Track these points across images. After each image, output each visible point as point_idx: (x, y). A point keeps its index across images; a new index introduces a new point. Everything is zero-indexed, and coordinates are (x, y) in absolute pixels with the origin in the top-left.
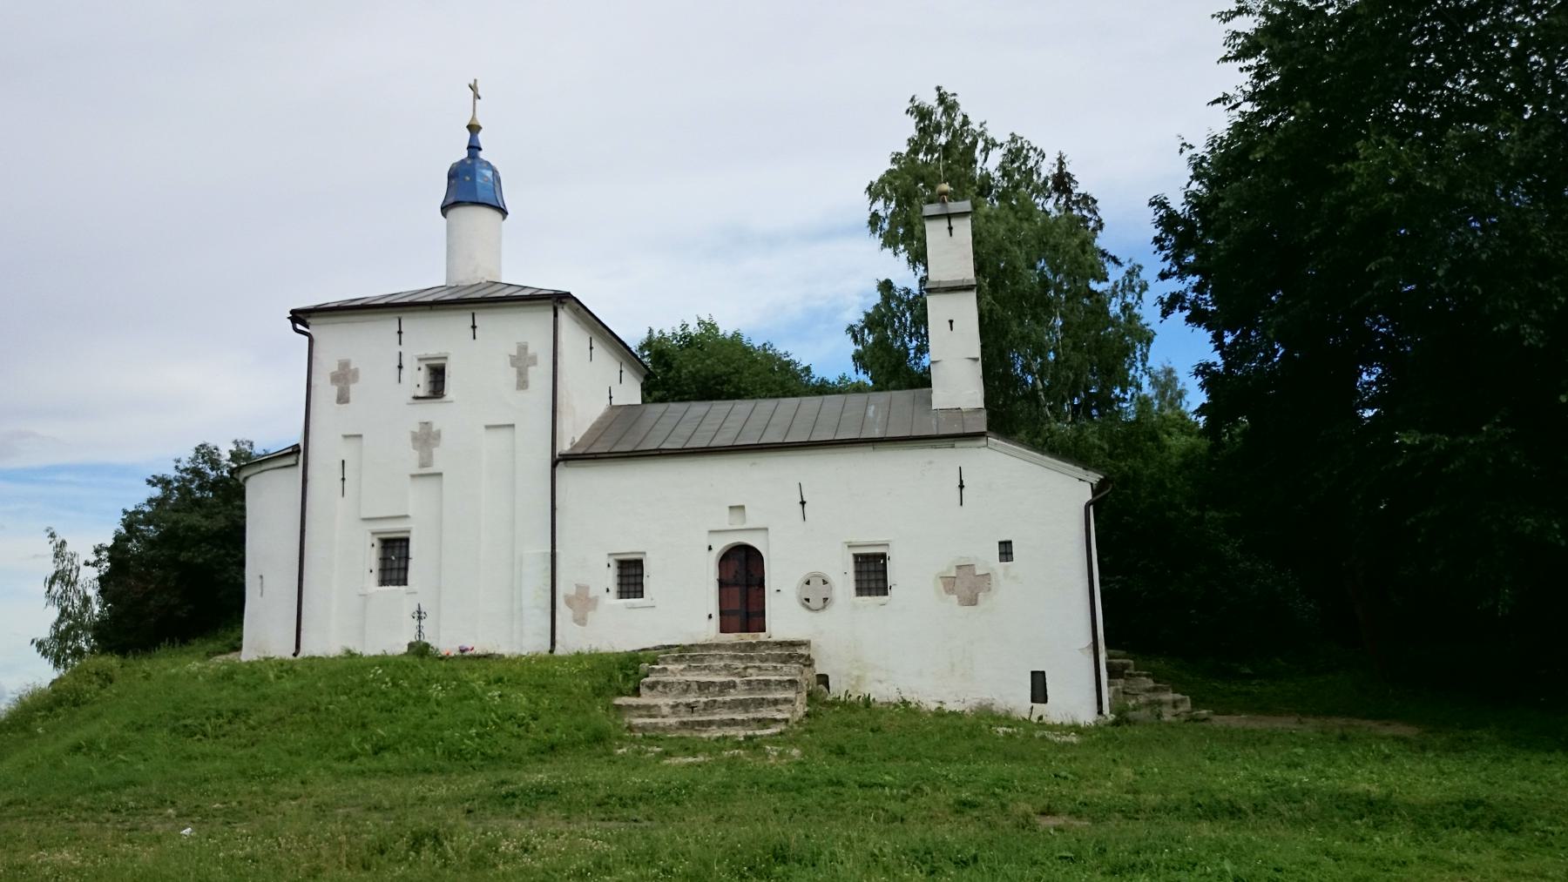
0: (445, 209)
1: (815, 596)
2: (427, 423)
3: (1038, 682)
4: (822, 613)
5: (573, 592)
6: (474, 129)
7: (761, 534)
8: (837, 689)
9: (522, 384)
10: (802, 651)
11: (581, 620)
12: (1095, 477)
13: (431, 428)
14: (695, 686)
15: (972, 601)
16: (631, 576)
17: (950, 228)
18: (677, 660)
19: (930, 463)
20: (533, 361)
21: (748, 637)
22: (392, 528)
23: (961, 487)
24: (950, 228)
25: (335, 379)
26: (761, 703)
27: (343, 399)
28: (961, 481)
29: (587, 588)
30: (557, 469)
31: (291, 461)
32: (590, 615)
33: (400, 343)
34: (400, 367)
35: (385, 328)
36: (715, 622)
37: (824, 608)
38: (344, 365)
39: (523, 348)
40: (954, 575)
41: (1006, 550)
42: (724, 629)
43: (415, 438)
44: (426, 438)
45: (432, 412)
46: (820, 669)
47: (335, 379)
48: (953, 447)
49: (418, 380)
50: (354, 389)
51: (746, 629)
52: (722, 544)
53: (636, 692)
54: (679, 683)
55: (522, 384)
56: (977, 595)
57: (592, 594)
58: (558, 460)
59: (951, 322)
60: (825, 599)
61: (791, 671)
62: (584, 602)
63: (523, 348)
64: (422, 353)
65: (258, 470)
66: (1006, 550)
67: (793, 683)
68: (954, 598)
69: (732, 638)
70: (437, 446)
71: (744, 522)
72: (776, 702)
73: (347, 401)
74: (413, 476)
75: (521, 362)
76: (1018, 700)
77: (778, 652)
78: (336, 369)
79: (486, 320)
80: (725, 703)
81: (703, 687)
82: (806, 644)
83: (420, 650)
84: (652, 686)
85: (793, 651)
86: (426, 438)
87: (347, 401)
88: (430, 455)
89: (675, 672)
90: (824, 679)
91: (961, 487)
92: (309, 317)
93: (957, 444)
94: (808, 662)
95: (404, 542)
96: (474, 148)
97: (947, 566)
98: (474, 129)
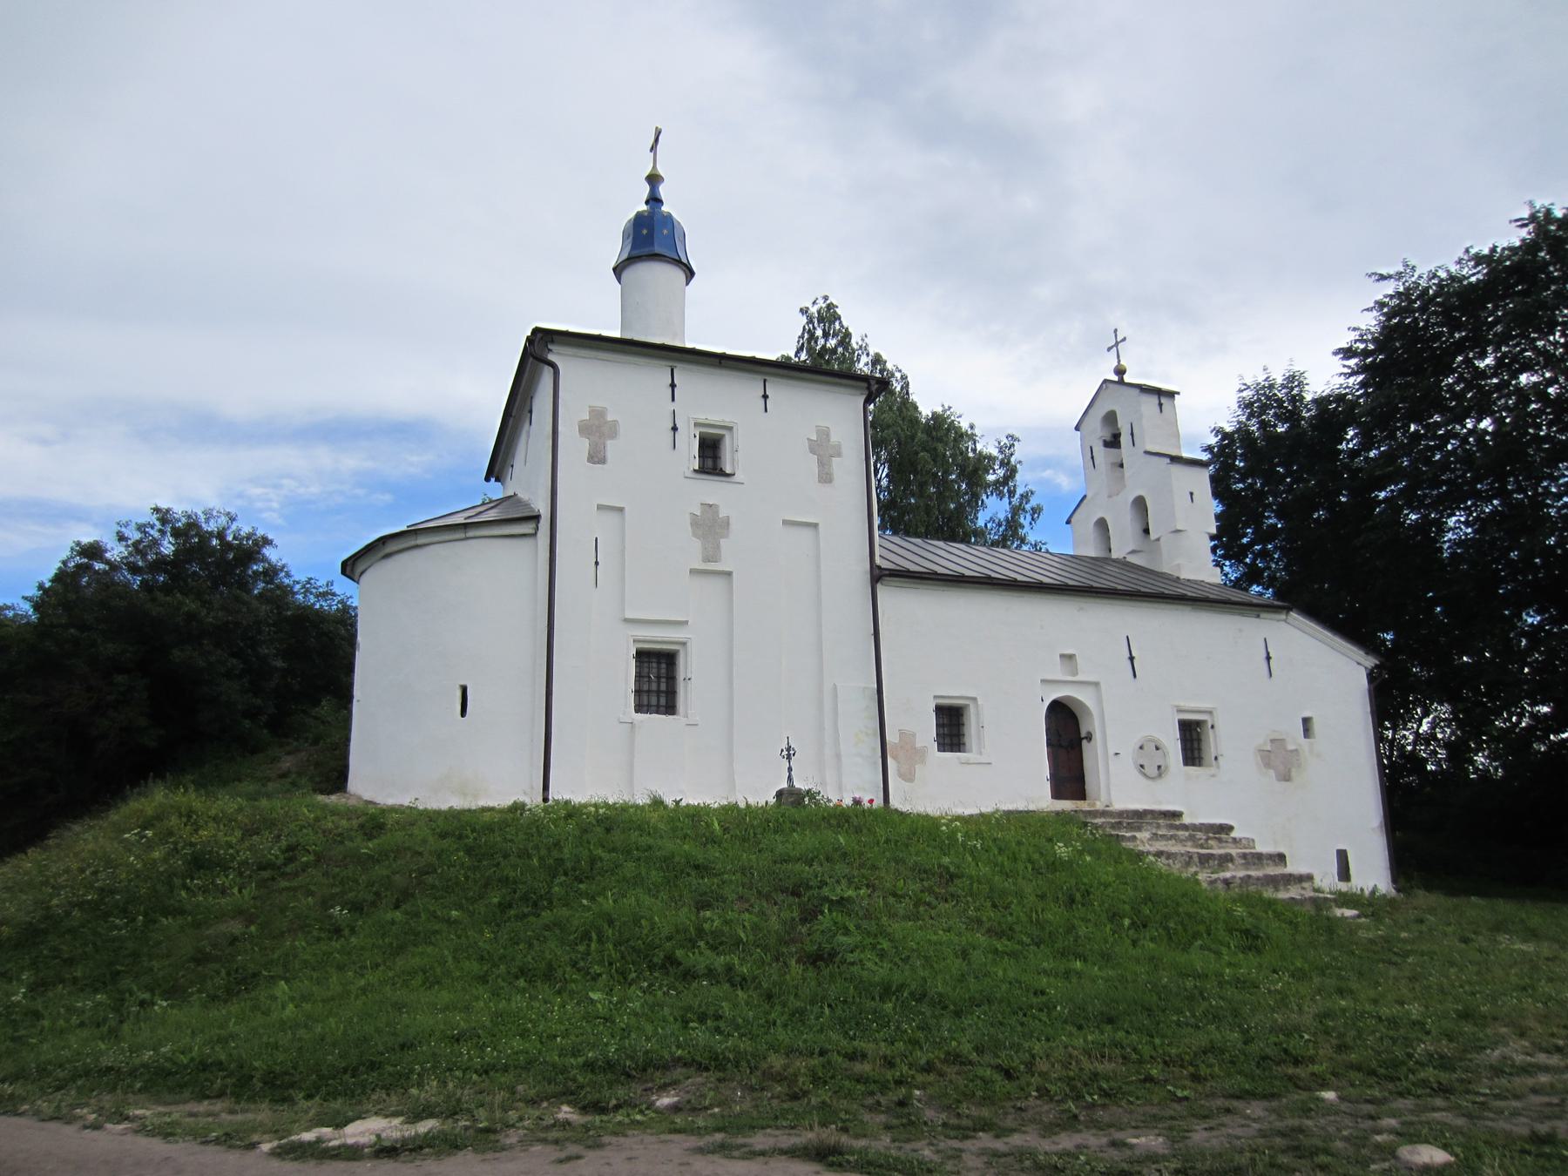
2: (711, 506)
4: (1149, 782)
6: (654, 179)
7: (1091, 689)
9: (826, 477)
11: (908, 777)
12: (1371, 662)
13: (717, 512)
14: (1196, 859)
17: (1161, 405)
19: (1240, 630)
22: (659, 637)
23: (1268, 658)
24: (1161, 405)
27: (597, 457)
28: (1268, 653)
29: (914, 735)
30: (879, 587)
31: (527, 528)
33: (673, 399)
34: (675, 429)
37: (1160, 775)
39: (824, 434)
40: (1269, 748)
42: (1057, 794)
43: (696, 522)
44: (710, 526)
45: (711, 490)
48: (1258, 616)
54: (1182, 855)
55: (826, 477)
56: (1289, 771)
59: (1192, 494)
60: (1159, 767)
62: (916, 755)
64: (702, 417)
65: (462, 535)
69: (1067, 805)
70: (726, 536)
71: (1075, 673)
73: (603, 461)
74: (693, 572)
75: (822, 450)
80: (1258, 879)
83: (790, 797)
86: (710, 526)
87: (603, 461)
88: (718, 547)
91: (1268, 658)
92: (552, 342)
93: (1263, 615)
96: (654, 200)
98: (654, 179)
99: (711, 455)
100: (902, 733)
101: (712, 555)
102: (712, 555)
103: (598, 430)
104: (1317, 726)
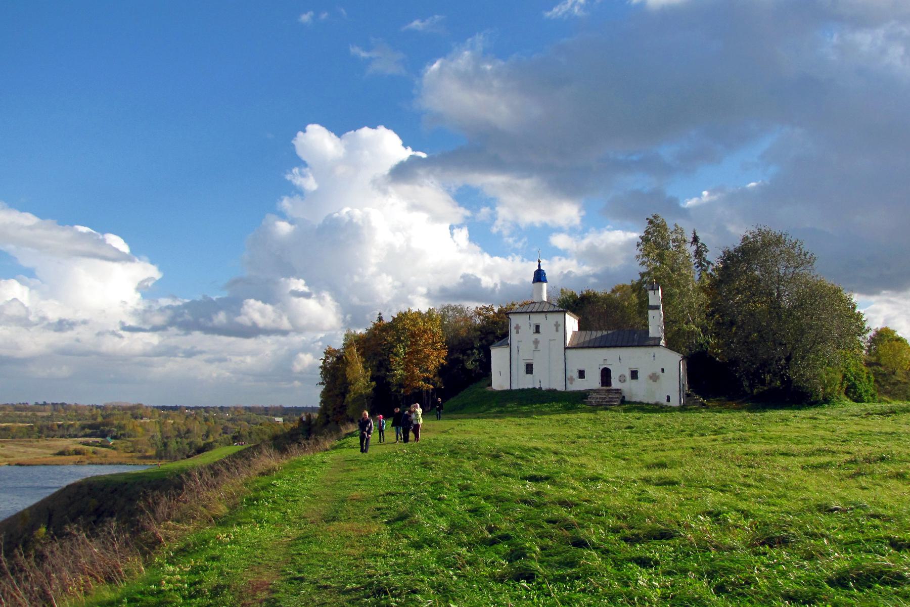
0: (534, 282)
1: (622, 379)
3: (668, 399)
5: (569, 377)
9: (557, 330)
11: (571, 383)
15: (655, 381)
16: (582, 374)
20: (560, 325)
21: (608, 388)
25: (515, 328)
26: (611, 401)
27: (517, 332)
32: (573, 382)
35: (527, 316)
36: (600, 385)
38: (517, 325)
39: (557, 322)
41: (663, 370)
42: (602, 386)
44: (536, 342)
45: (537, 336)
46: (623, 395)
47: (515, 328)
49: (533, 329)
50: (520, 330)
51: (607, 386)
52: (602, 367)
55: (557, 330)
58: (566, 348)
63: (557, 322)
64: (535, 323)
66: (663, 370)
67: (618, 398)
69: (604, 388)
75: (557, 325)
76: (664, 402)
78: (515, 326)
79: (549, 316)
81: (601, 398)
82: (620, 390)
84: (590, 398)
85: (618, 391)
86: (536, 342)
89: (594, 395)
90: (624, 397)
94: (621, 393)
96: (539, 266)
97: (650, 373)
99: (537, 329)
101: (536, 347)
102: (536, 347)
103: (517, 328)
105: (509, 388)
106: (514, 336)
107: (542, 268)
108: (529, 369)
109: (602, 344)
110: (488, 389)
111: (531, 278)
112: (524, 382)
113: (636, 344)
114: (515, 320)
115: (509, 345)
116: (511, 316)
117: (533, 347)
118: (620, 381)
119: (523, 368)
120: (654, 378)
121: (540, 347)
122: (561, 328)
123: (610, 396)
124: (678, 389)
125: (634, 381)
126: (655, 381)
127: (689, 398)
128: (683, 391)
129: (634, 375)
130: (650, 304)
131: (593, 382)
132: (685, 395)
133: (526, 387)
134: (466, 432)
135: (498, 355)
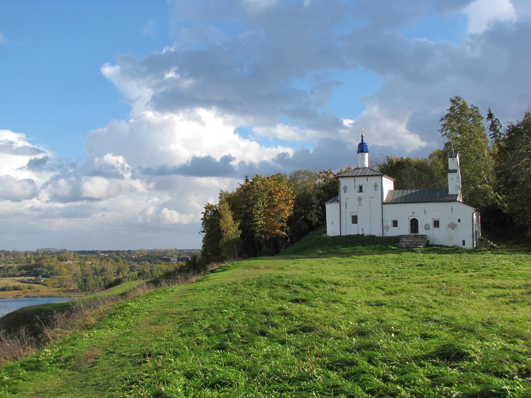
0: (358, 152)
1: (427, 227)
5: (386, 226)
6: (362, 137)
8: (431, 243)
9: (376, 190)
10: (425, 237)
11: (387, 231)
16: (395, 223)
17: (453, 160)
18: (405, 238)
20: (378, 186)
21: (416, 234)
22: (354, 214)
23: (452, 209)
24: (453, 160)
27: (345, 192)
32: (389, 230)
35: (352, 179)
36: (410, 231)
38: (345, 186)
39: (376, 184)
41: (459, 220)
42: (411, 232)
43: (358, 199)
44: (360, 199)
45: (360, 194)
46: (428, 240)
49: (357, 189)
51: (415, 232)
52: (411, 218)
53: (399, 243)
55: (376, 190)
57: (389, 226)
58: (383, 203)
60: (429, 228)
61: (422, 240)
62: (388, 228)
63: (376, 184)
64: (358, 184)
66: (459, 220)
67: (423, 242)
68: (450, 228)
69: (413, 234)
72: (420, 245)
73: (346, 192)
75: (376, 186)
76: (460, 245)
77: (421, 237)
78: (344, 187)
79: (369, 178)
81: (409, 242)
82: (425, 235)
84: (401, 242)
85: (423, 237)
86: (360, 199)
87: (346, 192)
90: (428, 241)
91: (452, 209)
94: (426, 238)
95: (356, 217)
96: (362, 140)
97: (449, 222)
98: (362, 137)
99: (361, 189)
100: (387, 225)
101: (360, 203)
102: (360, 203)
103: (345, 188)
104: (461, 221)
105: (339, 235)
106: (343, 195)
107: (364, 142)
108: (355, 220)
109: (407, 201)
110: (324, 235)
111: (357, 149)
112: (351, 230)
113: (438, 200)
114: (343, 182)
115: (339, 202)
116: (340, 179)
117: (357, 203)
118: (425, 228)
119: (350, 219)
120: (452, 226)
121: (362, 202)
122: (379, 188)
123: (417, 241)
124: (472, 236)
125: (436, 229)
126: (453, 229)
127: (481, 242)
128: (476, 237)
129: (436, 224)
130: (450, 168)
131: (404, 229)
132: (478, 240)
133: (352, 234)
134: (297, 269)
135: (331, 209)
